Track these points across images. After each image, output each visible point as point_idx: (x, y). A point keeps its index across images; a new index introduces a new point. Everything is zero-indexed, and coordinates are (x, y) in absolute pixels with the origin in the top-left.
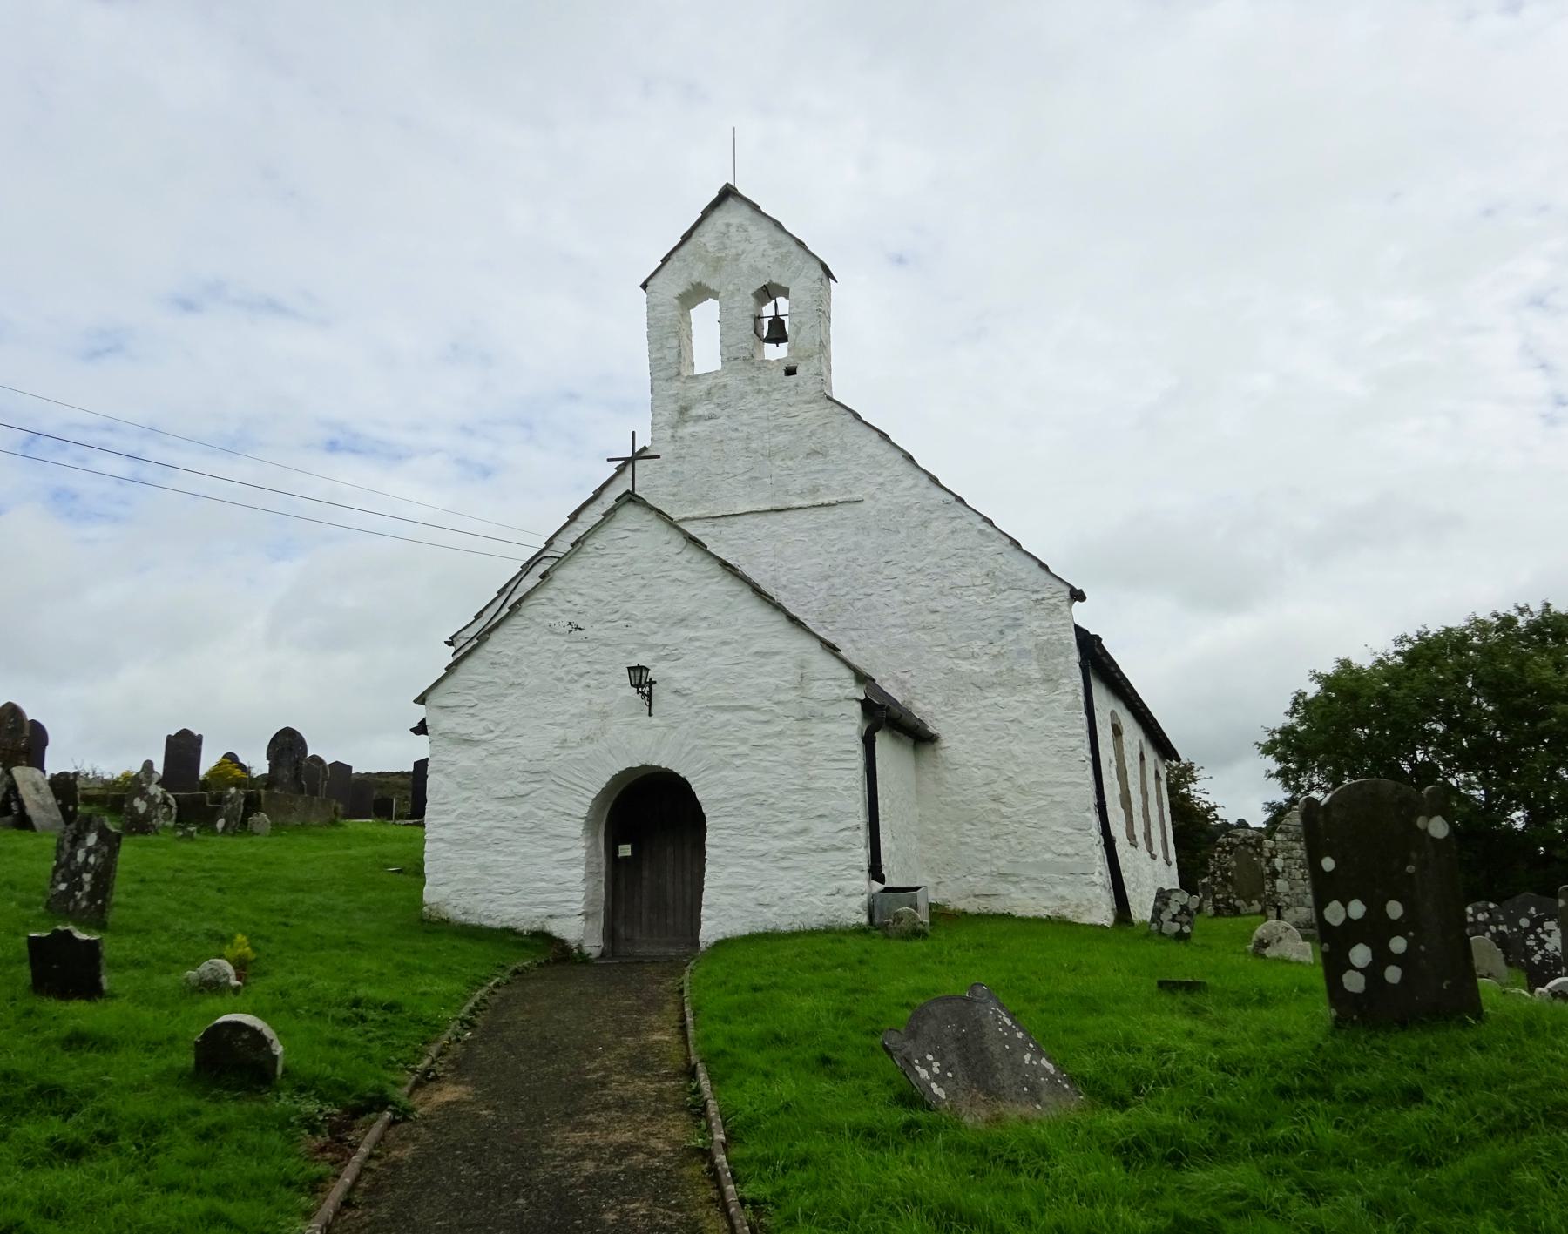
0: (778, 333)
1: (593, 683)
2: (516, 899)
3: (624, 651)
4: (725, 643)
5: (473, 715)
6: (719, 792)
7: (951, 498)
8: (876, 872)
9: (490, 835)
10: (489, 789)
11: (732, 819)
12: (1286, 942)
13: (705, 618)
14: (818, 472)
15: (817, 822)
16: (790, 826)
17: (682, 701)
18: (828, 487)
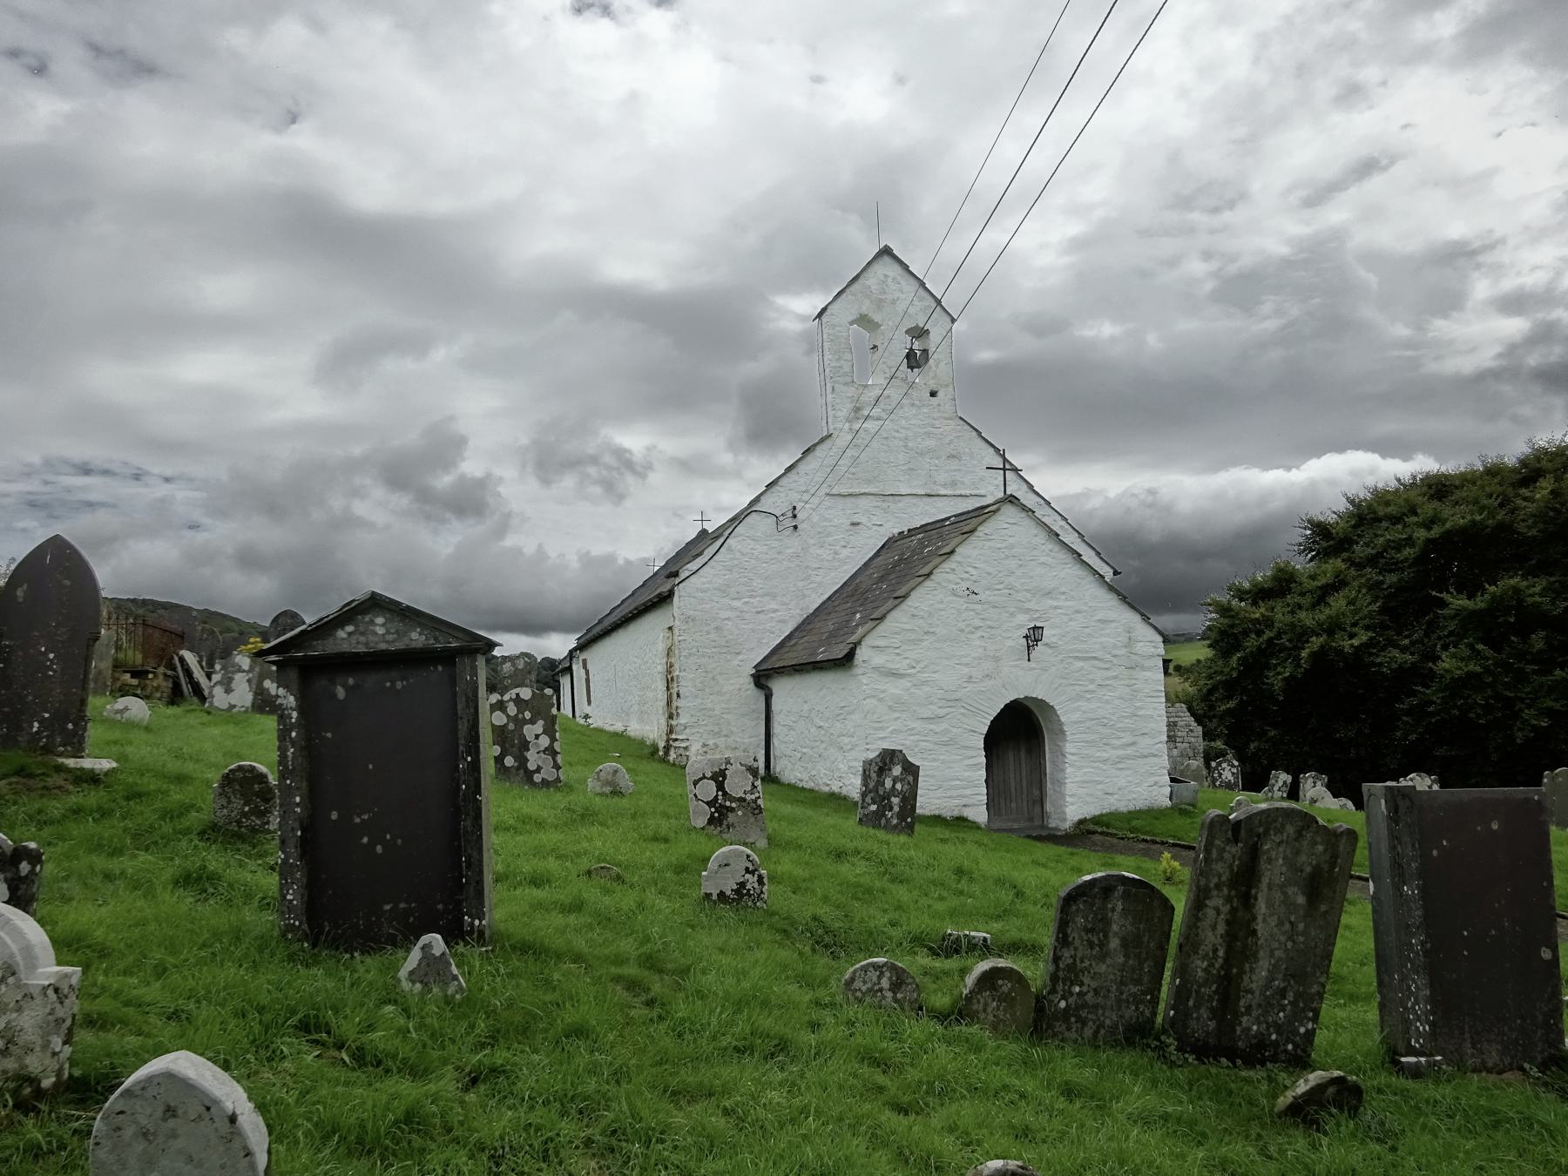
1: (984, 634)
2: (939, 793)
3: (1007, 612)
4: (1077, 612)
5: (898, 654)
6: (1076, 716)
7: (1042, 502)
9: (917, 746)
10: (915, 711)
11: (1084, 735)
12: (1326, 799)
13: (1064, 593)
14: (955, 471)
15: (1141, 738)
16: (1124, 740)
17: (1050, 651)
18: (963, 483)
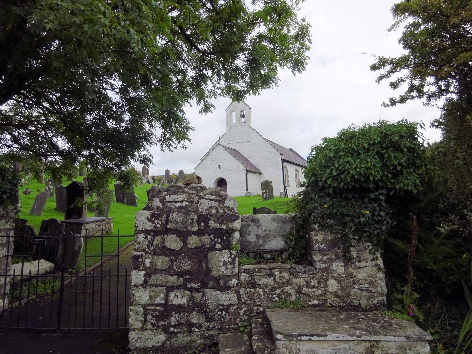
0: (244, 116)
8: (247, 190)
